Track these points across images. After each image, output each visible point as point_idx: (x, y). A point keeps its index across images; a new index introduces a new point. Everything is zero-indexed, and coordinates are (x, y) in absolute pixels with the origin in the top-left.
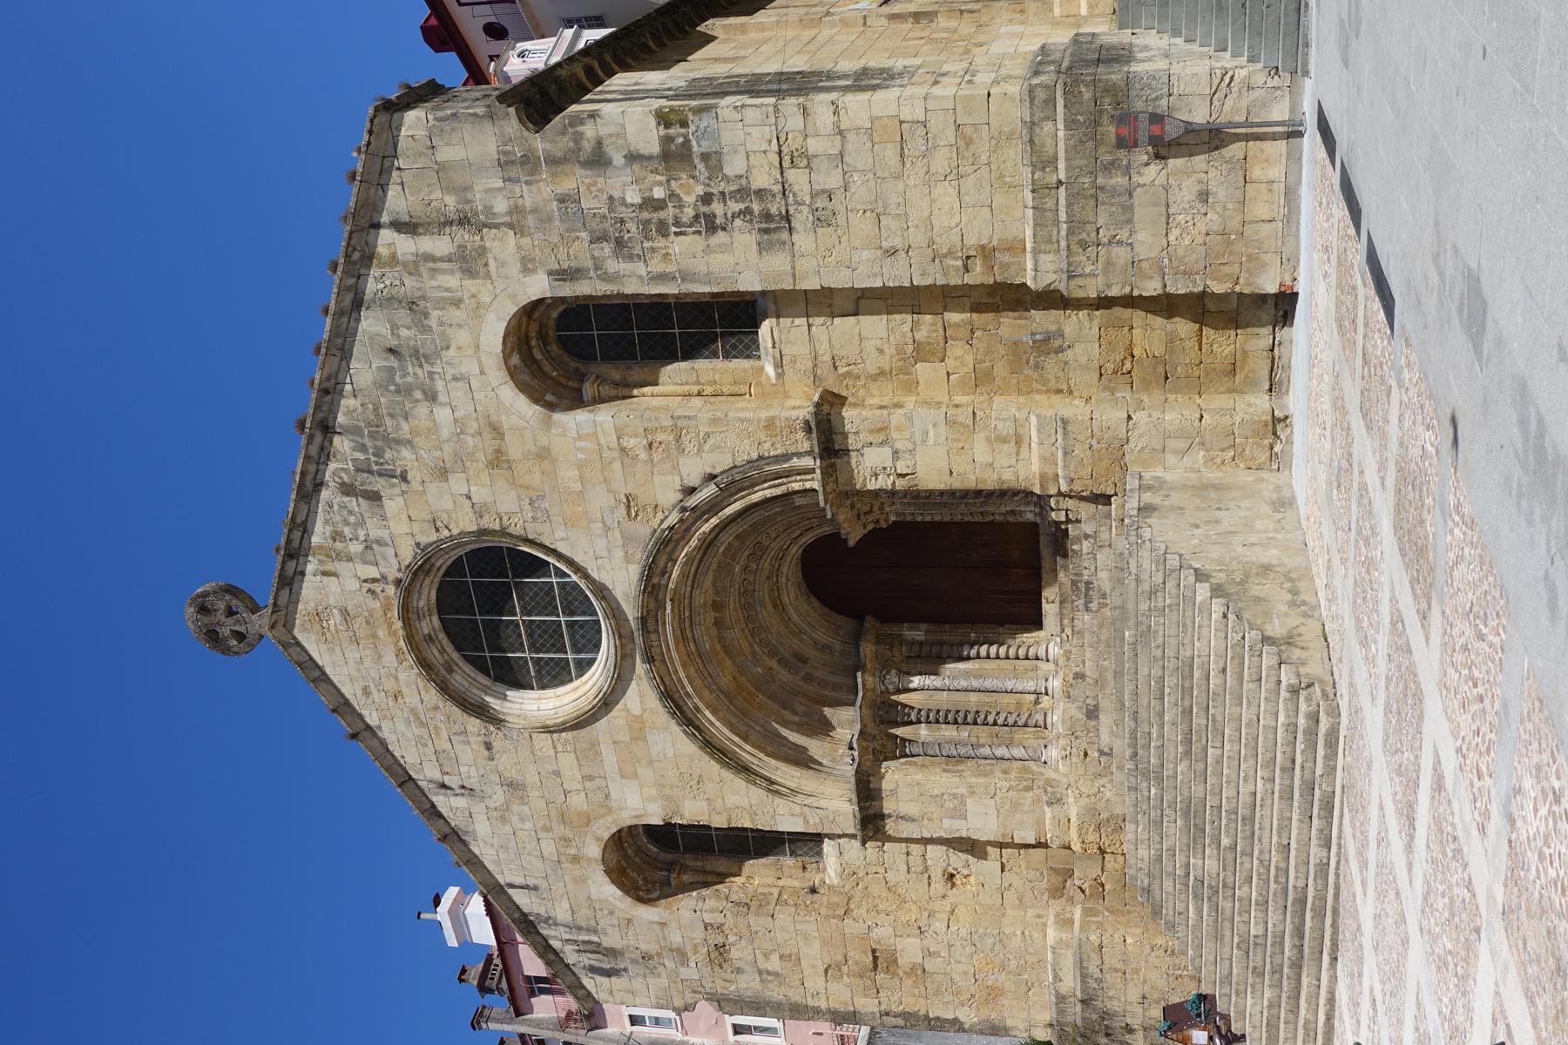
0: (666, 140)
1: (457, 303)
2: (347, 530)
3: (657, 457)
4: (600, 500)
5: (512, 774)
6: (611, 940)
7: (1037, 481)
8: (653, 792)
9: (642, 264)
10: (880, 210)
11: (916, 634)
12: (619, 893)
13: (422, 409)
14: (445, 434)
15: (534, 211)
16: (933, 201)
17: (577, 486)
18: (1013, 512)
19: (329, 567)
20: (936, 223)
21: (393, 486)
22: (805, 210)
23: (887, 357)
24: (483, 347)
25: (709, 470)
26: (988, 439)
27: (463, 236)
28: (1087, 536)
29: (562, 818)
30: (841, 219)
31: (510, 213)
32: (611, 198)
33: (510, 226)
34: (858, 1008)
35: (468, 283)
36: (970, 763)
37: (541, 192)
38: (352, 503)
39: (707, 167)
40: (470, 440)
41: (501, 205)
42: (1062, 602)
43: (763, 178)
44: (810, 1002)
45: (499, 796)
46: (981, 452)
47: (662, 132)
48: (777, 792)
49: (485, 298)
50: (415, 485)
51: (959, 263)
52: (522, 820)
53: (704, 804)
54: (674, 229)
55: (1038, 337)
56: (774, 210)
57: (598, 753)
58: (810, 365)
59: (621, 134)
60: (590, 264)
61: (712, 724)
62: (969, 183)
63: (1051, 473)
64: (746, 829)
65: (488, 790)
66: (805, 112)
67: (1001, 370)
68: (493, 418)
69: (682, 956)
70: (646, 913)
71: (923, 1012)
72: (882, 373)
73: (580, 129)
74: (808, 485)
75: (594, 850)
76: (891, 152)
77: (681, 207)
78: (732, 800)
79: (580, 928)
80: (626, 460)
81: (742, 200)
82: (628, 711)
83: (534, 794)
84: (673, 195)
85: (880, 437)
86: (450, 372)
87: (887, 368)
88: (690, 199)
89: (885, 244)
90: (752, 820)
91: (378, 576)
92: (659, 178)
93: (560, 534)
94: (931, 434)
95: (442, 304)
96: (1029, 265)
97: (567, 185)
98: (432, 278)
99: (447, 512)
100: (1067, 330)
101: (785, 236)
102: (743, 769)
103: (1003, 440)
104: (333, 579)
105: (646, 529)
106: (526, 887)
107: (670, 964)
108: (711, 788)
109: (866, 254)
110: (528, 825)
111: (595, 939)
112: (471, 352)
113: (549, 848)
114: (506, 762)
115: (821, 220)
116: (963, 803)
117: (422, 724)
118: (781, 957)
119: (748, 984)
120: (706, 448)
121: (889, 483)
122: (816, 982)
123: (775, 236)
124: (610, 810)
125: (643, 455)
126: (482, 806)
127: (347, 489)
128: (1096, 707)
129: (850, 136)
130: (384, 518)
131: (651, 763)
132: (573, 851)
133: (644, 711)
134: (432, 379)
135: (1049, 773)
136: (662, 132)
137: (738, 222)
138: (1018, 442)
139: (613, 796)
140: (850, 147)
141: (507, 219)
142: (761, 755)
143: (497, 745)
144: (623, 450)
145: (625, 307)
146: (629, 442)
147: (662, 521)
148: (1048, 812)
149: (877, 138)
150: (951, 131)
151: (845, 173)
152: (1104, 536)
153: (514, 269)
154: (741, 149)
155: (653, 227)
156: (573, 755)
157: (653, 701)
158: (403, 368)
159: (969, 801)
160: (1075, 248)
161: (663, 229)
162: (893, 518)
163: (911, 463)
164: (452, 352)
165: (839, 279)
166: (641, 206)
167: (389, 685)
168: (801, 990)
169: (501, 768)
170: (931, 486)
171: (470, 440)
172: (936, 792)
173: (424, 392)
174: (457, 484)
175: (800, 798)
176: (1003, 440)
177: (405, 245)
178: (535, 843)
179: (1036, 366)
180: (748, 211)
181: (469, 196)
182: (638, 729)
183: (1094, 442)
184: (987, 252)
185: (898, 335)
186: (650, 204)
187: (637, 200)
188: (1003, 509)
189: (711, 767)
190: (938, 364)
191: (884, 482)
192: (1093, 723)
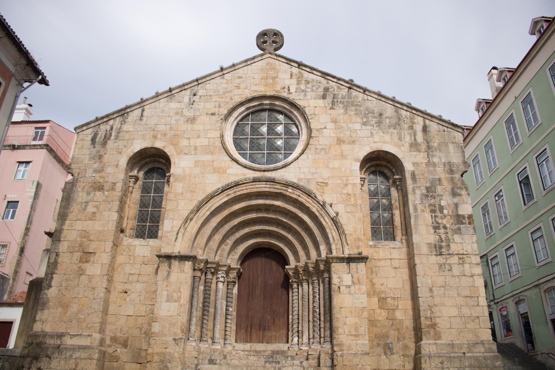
0: (463, 217)
1: (400, 139)
2: (310, 86)
3: (344, 196)
4: (325, 173)
5: (199, 120)
6: (110, 144)
7: (339, 343)
9: (419, 202)
10: (446, 288)
11: (235, 291)
12: (136, 151)
13: (359, 120)
14: (350, 125)
15: (435, 170)
16: (451, 307)
17: (331, 166)
19: (294, 76)
20: (443, 308)
21: (329, 104)
22: (444, 261)
23: (380, 287)
24: (384, 144)
25: (339, 215)
26: (356, 323)
27: (424, 147)
29: (176, 136)
30: (441, 273)
31: (433, 162)
32: (442, 196)
33: (429, 161)
34: (62, 243)
35: (407, 145)
37: (441, 173)
38: (321, 90)
39: (456, 229)
40: (348, 133)
41: (436, 160)
43: (454, 248)
44: (67, 222)
45: (189, 114)
46: (351, 320)
47: (466, 216)
49: (402, 148)
50: (329, 112)
51: (429, 315)
52: (176, 120)
53: (180, 191)
54: (433, 215)
55: (391, 345)
56: (443, 250)
57: (208, 154)
58: (376, 258)
59: (463, 202)
60: (418, 185)
61: (221, 200)
62: (458, 320)
65: (192, 110)
66: (477, 264)
67: (375, 330)
68: (357, 142)
69: (99, 171)
70: (123, 161)
71: (56, 271)
72: (373, 285)
73: (464, 190)
75: (159, 144)
76: (467, 293)
77: (441, 218)
78: (182, 204)
79: (119, 133)
80: (342, 185)
81: (446, 240)
83: (189, 126)
84: (445, 216)
85: (356, 281)
86: (374, 132)
87: (375, 287)
88: (444, 222)
89: (434, 289)
91: (291, 91)
92: (451, 213)
93: (310, 156)
95: (399, 134)
96: (430, 342)
97: (445, 182)
98: (408, 133)
99: (319, 119)
100: (394, 356)
101: (434, 253)
102: (198, 208)
104: (289, 77)
105: (312, 187)
106: (142, 116)
107: (96, 166)
109: (430, 281)
110: (173, 122)
111: (112, 138)
112: (382, 140)
113: (162, 128)
114: (205, 119)
115: (440, 266)
116: (175, 301)
117: (224, 93)
118: (94, 213)
119: (80, 196)
122: (79, 226)
123: (434, 249)
124: (179, 154)
125: (344, 191)
126: (184, 107)
127: (326, 89)
129: (471, 279)
130: (315, 99)
131: (202, 173)
132: (159, 136)
133: (228, 174)
134: (371, 125)
136: (466, 216)
137: (438, 237)
138: (355, 336)
139: (186, 156)
140: (468, 278)
141: (431, 161)
143: (213, 117)
146: (350, 188)
148: (171, 338)
149: (472, 288)
150: (476, 315)
151: (458, 276)
153: (415, 160)
154: (463, 241)
155: (433, 208)
156: (207, 144)
157: (232, 179)
158: (375, 117)
159: (177, 304)
160: (441, 359)
161: (433, 211)
163: (345, 292)
164: (381, 134)
165: (419, 270)
166: (440, 205)
167: (243, 86)
168: (75, 219)
169: (202, 117)
171: (348, 133)
172: (182, 290)
173: (366, 122)
174: (330, 125)
176: (356, 329)
177: (419, 128)
178: (164, 123)
179: (378, 345)
180: (442, 241)
181: (438, 151)
184: (433, 326)
185: (389, 291)
186: (441, 209)
187: (442, 205)
189: (201, 196)
191: (335, 280)
192: (207, 362)
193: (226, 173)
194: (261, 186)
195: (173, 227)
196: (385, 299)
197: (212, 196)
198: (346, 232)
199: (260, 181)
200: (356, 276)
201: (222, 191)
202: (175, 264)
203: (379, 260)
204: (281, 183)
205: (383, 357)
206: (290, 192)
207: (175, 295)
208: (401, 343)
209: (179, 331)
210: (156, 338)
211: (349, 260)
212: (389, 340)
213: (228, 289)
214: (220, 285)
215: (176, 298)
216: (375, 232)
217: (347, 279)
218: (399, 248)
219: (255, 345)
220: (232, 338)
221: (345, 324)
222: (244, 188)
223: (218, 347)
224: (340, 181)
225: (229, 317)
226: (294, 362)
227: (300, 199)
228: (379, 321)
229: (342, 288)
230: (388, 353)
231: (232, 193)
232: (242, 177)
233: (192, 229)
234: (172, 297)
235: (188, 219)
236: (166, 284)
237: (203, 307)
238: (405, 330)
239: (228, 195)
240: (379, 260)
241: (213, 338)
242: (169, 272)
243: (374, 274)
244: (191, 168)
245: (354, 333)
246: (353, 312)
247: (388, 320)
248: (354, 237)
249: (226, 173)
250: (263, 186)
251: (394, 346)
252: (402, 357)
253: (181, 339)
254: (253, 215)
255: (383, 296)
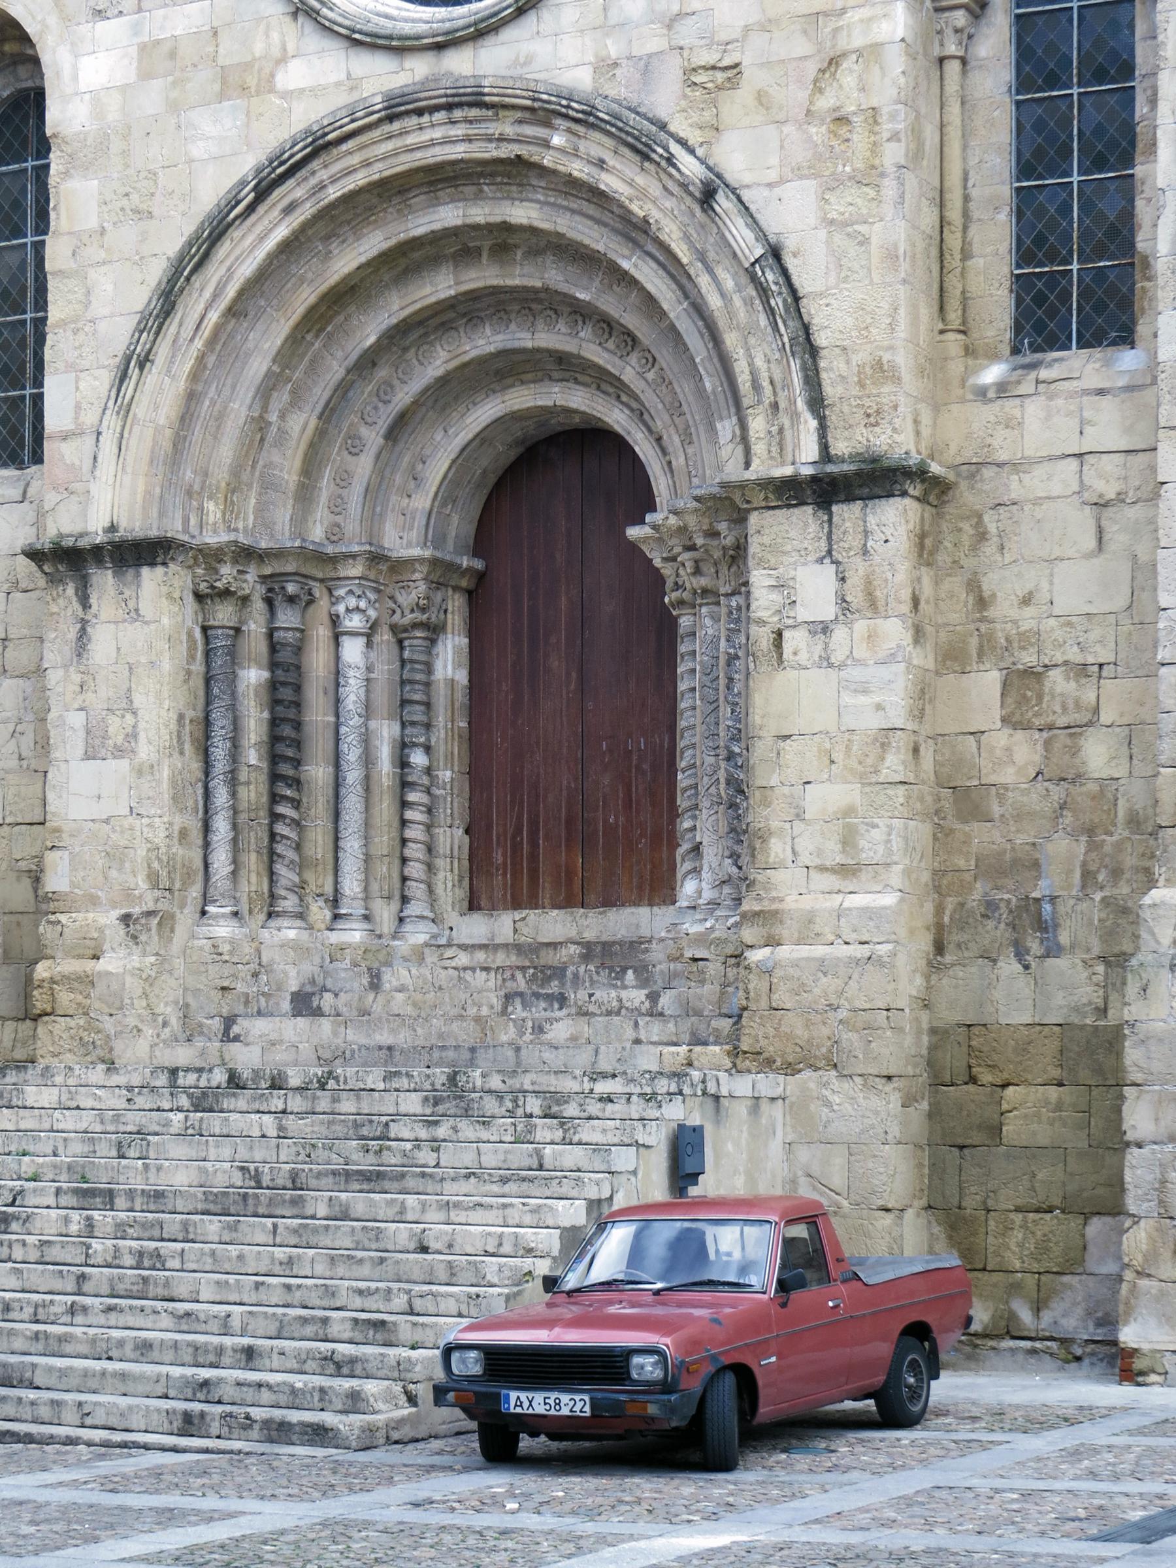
3: (818, 132)
7: (766, 905)
8: (113, 115)
11: (450, 662)
18: (697, 849)
23: (1014, 613)
26: (849, 811)
28: (653, 997)
36: (196, 766)
42: (518, 948)
46: (829, 796)
48: (123, 376)
53: (93, 223)
58: (1003, 456)
61: (262, 238)
63: (786, 931)
64: (41, 303)
74: (759, 448)
78: (104, 282)
82: (282, 60)
85: (856, 597)
90: (63, 323)
94: (863, 699)
102: (168, 300)
103: (848, 841)
108: (125, 236)
116: (119, 752)
120: (838, 238)
121: (763, 614)
125: (824, 103)
128: (318, 1013)
133: (286, 95)
135: (185, 918)
142: (199, 344)
144: (834, 62)
145: (1127, 69)
146: (848, 76)
147: (683, 143)
152: (654, 1030)
157: (305, 116)
159: (123, 765)
162: (685, 622)
163: (803, 658)
170: (758, 699)
172: (139, 700)
175: (112, 422)
176: (848, 841)
182: (240, 83)
183: (843, 1014)
185: (1059, 634)
188: (705, 836)
189: (172, 236)
190: (997, 714)
192: (286, 1006)
193: (272, 90)
194: (426, 136)
195: (78, 407)
196: (1034, 675)
197: (216, 231)
198: (821, 339)
199: (420, 112)
200: (857, 570)
201: (263, 192)
202: (104, 580)
203: (1017, 466)
204: (514, 107)
205: (1009, 966)
206: (560, 149)
207: (116, 727)
208: (1098, 896)
209: (142, 883)
210: (63, 918)
211: (826, 490)
212: (1042, 883)
213: (403, 662)
214: (353, 651)
215: (120, 740)
216: (1040, 299)
217: (816, 590)
218: (1129, 388)
219: (532, 915)
220: (449, 885)
221: (799, 816)
222: (355, 159)
223: (354, 935)
224: (801, 47)
225: (412, 797)
226: (624, 994)
227: (609, 182)
228: (1002, 790)
229: (793, 640)
230: (1035, 947)
231: (303, 197)
232: (341, 99)
233: (156, 408)
234: (105, 737)
235: (134, 362)
236: (77, 678)
237: (262, 761)
238: (1121, 832)
239: (289, 209)
240: (1017, 466)
241: (335, 902)
242: (84, 623)
243: (990, 548)
244: (124, 89)
245: (839, 859)
246: (838, 756)
247: (1040, 786)
248: (856, 359)
249: (272, 90)
250: (438, 133)
251: (1061, 909)
252: (1100, 969)
253: (150, 914)
254: (440, 286)
255: (1028, 658)
